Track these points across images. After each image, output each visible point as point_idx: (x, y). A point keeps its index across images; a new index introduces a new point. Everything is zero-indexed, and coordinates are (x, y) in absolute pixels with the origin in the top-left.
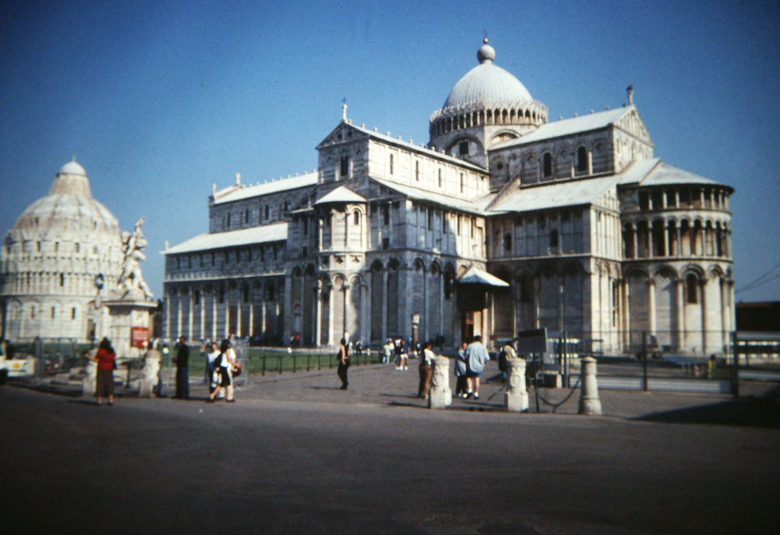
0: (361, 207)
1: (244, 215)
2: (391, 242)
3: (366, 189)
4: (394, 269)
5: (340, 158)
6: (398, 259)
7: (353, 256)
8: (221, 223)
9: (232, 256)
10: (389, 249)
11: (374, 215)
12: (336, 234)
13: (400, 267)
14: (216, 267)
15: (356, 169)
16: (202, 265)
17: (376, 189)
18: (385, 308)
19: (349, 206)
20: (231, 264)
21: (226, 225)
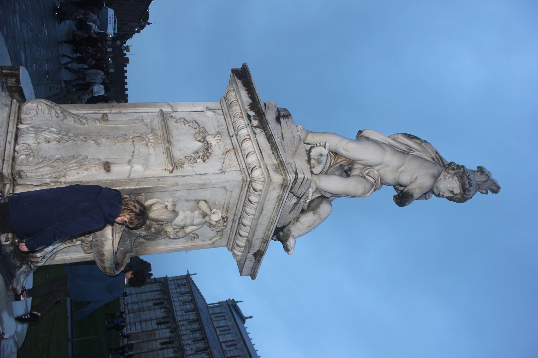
1: (226, 328)
9: (195, 326)
14: (184, 314)
16: (184, 303)
20: (189, 327)
21: (216, 315)
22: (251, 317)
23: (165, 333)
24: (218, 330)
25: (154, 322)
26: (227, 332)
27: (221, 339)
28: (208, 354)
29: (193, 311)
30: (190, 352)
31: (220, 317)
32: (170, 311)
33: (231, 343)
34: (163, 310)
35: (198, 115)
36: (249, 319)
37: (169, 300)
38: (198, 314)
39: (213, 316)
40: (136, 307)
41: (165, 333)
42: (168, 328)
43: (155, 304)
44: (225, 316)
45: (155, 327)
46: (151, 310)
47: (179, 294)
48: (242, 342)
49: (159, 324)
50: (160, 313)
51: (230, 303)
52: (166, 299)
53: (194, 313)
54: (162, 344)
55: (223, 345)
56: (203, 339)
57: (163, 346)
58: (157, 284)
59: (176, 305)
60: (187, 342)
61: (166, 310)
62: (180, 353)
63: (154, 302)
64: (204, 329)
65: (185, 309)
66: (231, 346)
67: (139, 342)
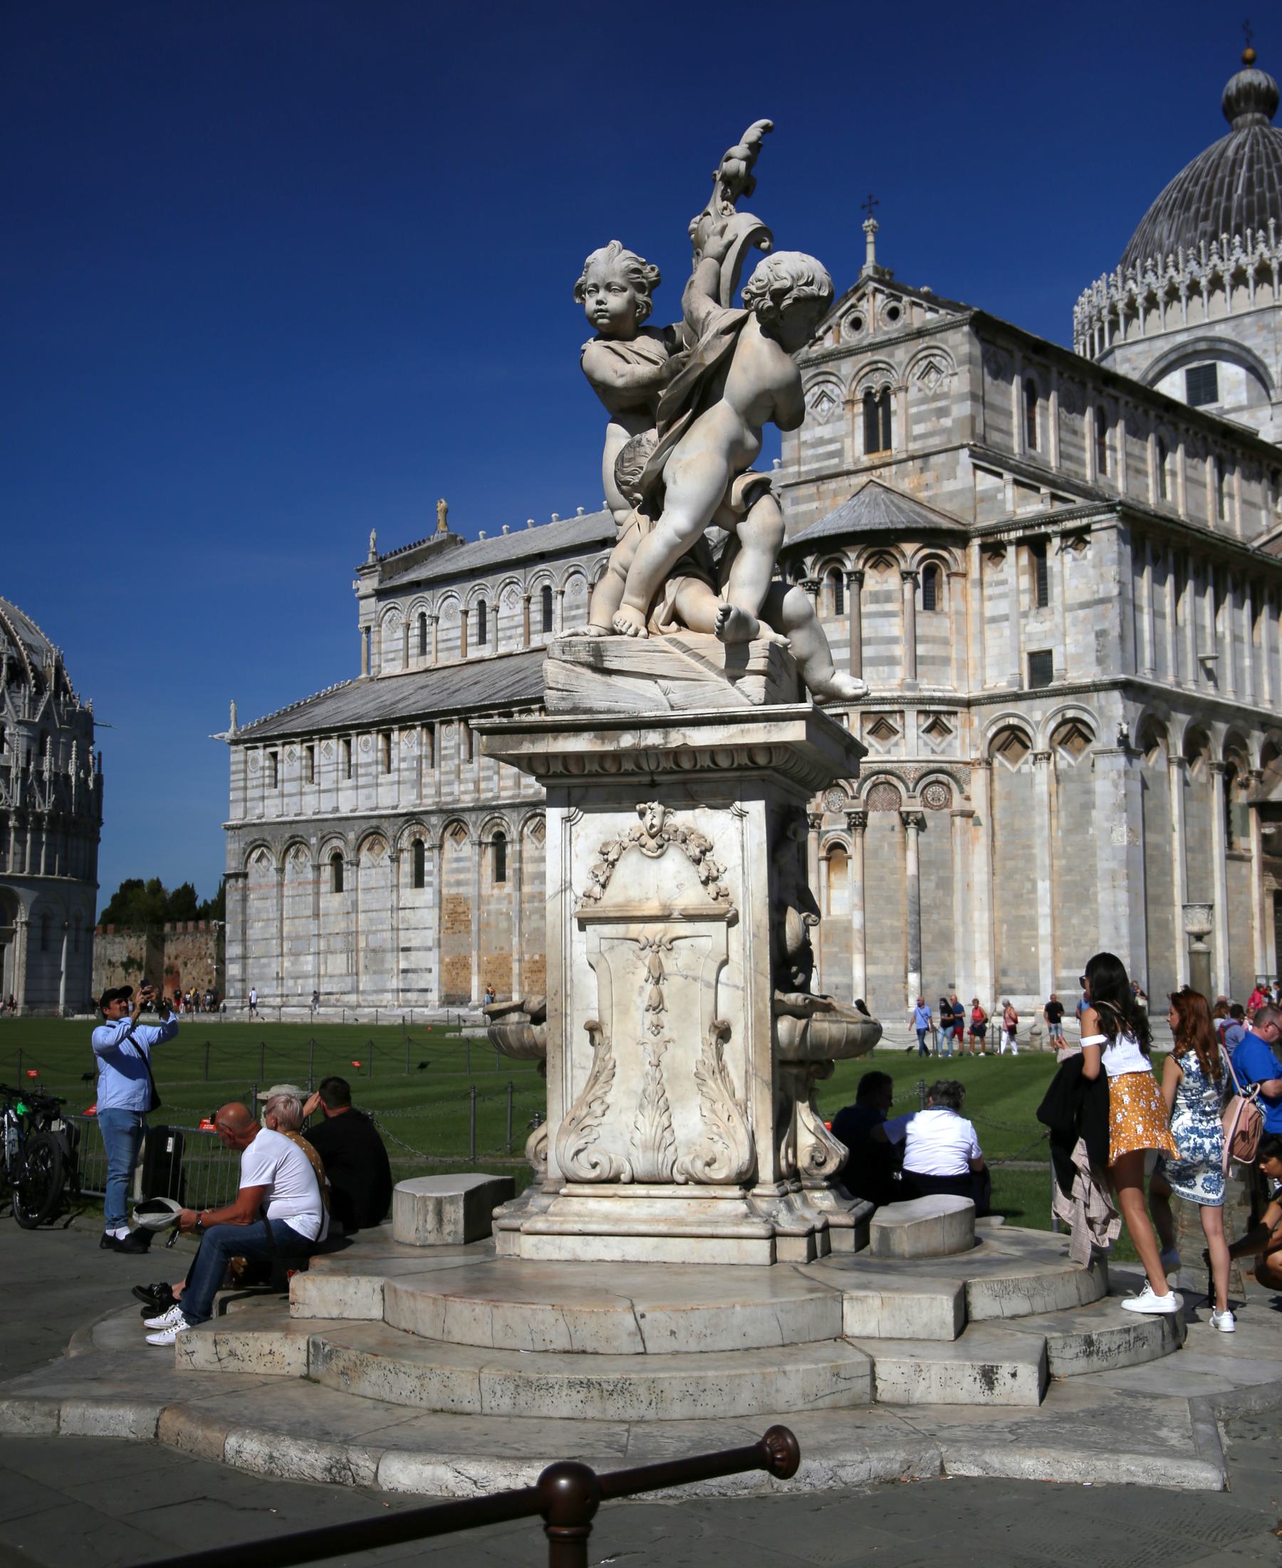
0: (950, 553)
1: (473, 620)
2: (1057, 663)
4: (1075, 752)
5: (860, 395)
7: (927, 713)
8: (401, 644)
10: (1054, 684)
11: (990, 574)
12: (870, 642)
13: (1096, 745)
14: (393, 777)
15: (918, 429)
16: (350, 770)
18: (1043, 887)
21: (414, 651)
23: (458, 860)
24: (473, 654)
25: (409, 895)
27: (516, 646)
29: (388, 738)
31: (423, 635)
32: (373, 831)
34: (365, 857)
35: (581, 840)
37: (331, 827)
39: (416, 664)
40: (338, 963)
41: (458, 860)
42: (441, 847)
43: (339, 888)
45: (427, 895)
46: (355, 904)
47: (308, 788)
49: (419, 881)
50: (373, 872)
52: (324, 840)
53: (395, 736)
54: (500, 876)
57: (509, 872)
58: (252, 866)
59: (348, 802)
61: (366, 845)
63: (326, 887)
67: (479, 966)
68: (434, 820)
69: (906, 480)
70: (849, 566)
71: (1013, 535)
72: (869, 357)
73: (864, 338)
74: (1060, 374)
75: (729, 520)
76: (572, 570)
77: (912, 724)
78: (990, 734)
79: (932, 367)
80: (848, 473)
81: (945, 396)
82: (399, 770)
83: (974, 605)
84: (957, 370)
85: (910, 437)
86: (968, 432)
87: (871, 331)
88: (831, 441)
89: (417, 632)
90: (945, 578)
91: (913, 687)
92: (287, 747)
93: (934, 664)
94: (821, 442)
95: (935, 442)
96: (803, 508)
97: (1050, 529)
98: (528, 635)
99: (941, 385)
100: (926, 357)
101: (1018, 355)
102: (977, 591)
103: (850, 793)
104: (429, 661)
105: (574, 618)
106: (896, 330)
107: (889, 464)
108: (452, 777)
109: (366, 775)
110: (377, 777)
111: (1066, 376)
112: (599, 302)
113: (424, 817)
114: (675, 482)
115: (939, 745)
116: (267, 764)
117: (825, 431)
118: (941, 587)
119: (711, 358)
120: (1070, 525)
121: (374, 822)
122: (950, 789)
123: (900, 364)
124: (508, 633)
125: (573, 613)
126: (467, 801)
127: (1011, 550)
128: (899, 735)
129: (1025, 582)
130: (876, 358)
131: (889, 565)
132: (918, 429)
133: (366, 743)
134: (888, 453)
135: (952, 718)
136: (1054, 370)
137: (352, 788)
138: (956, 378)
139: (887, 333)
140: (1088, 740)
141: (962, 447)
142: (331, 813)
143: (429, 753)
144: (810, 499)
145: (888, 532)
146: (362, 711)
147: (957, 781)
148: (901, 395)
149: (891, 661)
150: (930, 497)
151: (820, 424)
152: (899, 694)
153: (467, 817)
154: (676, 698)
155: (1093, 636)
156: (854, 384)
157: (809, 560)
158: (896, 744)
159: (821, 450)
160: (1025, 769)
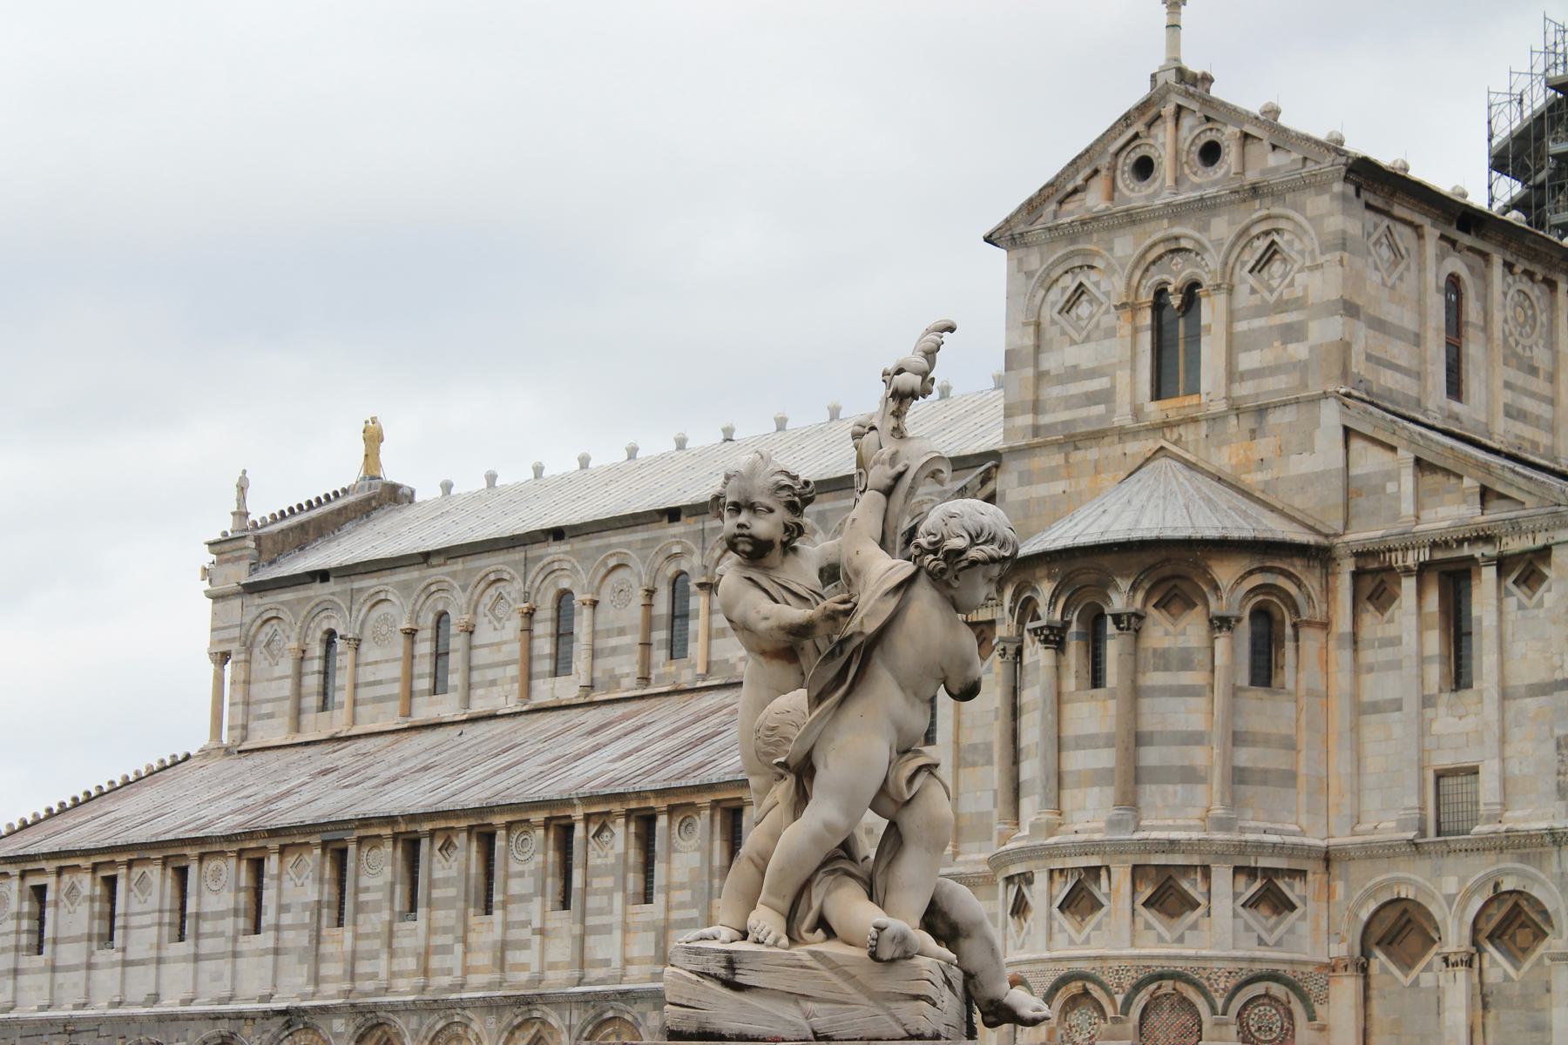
0: (1299, 584)
1: (424, 648)
2: (1488, 788)
3: (1321, 476)
4: (1516, 955)
5: (1146, 296)
6: (1546, 892)
7: (1251, 872)
8: (287, 687)
9: (377, 872)
14: (266, 939)
15: (1248, 361)
17: (1393, 476)
19: (1226, 572)
20: (374, 921)
21: (312, 701)
22: (373, 438)
24: (425, 710)
26: (457, 643)
27: (504, 698)
28: (602, 823)
29: (257, 867)
30: (560, 950)
31: (326, 674)
33: (544, 629)
36: (386, 452)
38: (290, 839)
44: (330, 637)
47: (102, 956)
48: (555, 549)
51: (240, 574)
53: (272, 865)
55: (546, 690)
56: (487, 839)
60: (482, 959)
62: (554, 1019)
64: (412, 818)
65: (228, 925)
66: (563, 635)
68: (339, 1025)
69: (1225, 451)
70: (1118, 602)
71: (1411, 560)
72: (1163, 229)
73: (1156, 194)
74: (1509, 266)
75: (890, 807)
76: (612, 562)
77: (1224, 893)
78: (1365, 915)
79: (1272, 252)
80: (1123, 433)
81: (1298, 304)
82: (277, 928)
83: (1341, 680)
84: (1320, 260)
85: (1232, 375)
86: (1337, 371)
87: (1169, 182)
88: (1092, 374)
89: (317, 665)
90: (1289, 631)
91: (1224, 824)
92: (66, 877)
93: (1264, 782)
94: (1075, 374)
95: (1277, 384)
96: (1040, 490)
97: (1478, 551)
98: (528, 677)
99: (1291, 284)
100: (1267, 233)
101: (1432, 233)
102: (1347, 654)
103: (1110, 1012)
104: (338, 722)
105: (614, 651)
106: (1214, 184)
107: (1195, 420)
108: (376, 944)
109: (214, 935)
110: (235, 939)
111: (1518, 269)
112: (740, 526)
113: (319, 1022)
114: (826, 766)
115: (1271, 930)
116: (26, 907)
117: (1082, 356)
118: (1281, 645)
119: (871, 627)
120: (1514, 545)
121: (224, 1027)
122: (1290, 1014)
123: (1218, 244)
124: (490, 674)
125: (614, 642)
126: (405, 991)
127: (1409, 585)
128: (1201, 910)
129: (1434, 641)
130: (1177, 231)
131: (1190, 605)
132: (1247, 361)
133: (218, 870)
134: (1194, 400)
135: (1297, 884)
136: (1497, 260)
137: (185, 959)
138: (1318, 273)
139: (1199, 187)
140: (1540, 935)
141: (1325, 395)
142: (144, 1005)
143: (335, 898)
144: (1052, 475)
145: (1189, 544)
146: (211, 812)
147: (1304, 998)
148: (1220, 299)
149: (1189, 776)
150: (1266, 483)
151: (1073, 342)
152: (1202, 835)
153: (400, 1022)
154: (822, 1023)
155: (1552, 745)
156: (1138, 274)
157: (1045, 589)
158: (1194, 927)
159: (1076, 388)
160: (1427, 980)
